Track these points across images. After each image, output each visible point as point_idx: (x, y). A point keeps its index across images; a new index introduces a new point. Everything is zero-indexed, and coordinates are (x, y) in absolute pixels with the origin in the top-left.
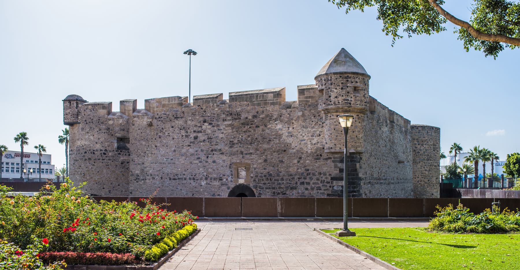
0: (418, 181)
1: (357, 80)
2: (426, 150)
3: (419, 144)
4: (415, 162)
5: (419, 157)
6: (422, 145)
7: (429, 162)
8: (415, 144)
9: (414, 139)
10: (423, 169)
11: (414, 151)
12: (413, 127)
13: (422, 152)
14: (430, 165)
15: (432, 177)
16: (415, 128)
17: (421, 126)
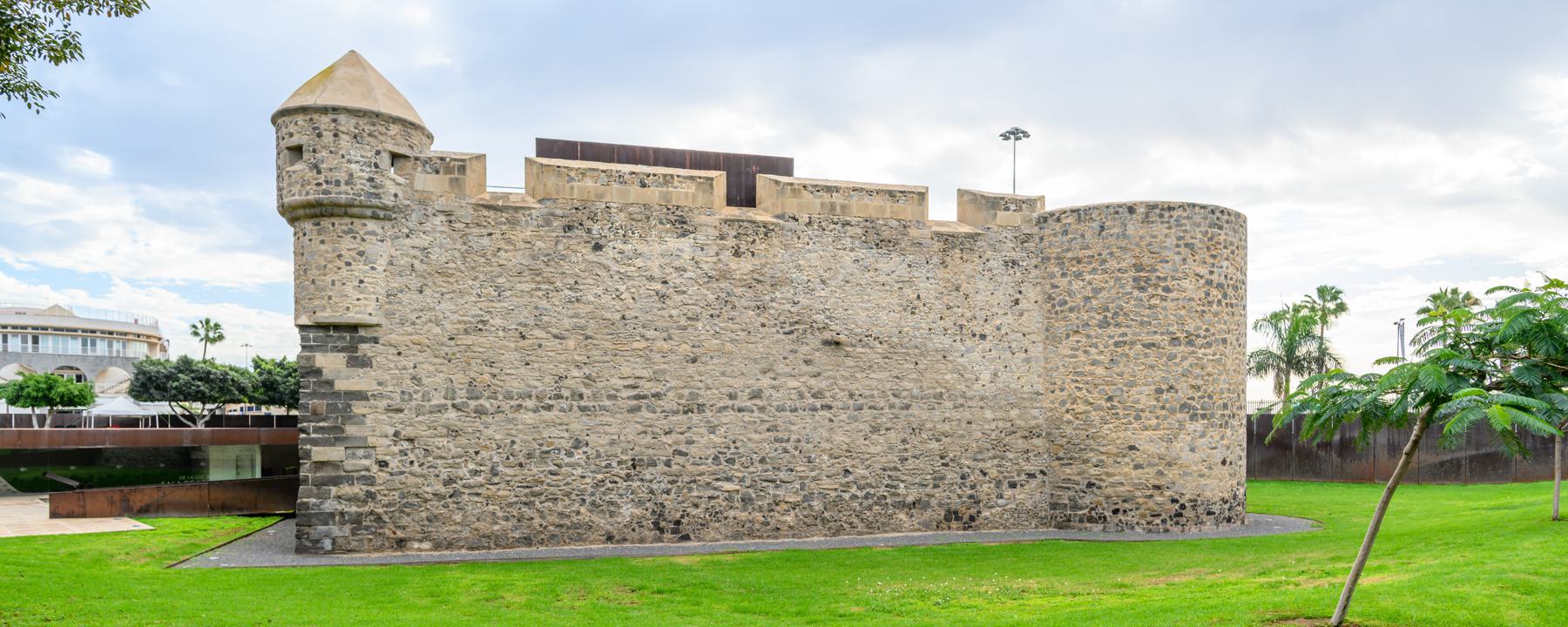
0: (1063, 403)
1: (292, 128)
2: (1097, 291)
3: (1064, 275)
4: (1051, 338)
5: (1064, 319)
6: (1078, 275)
7: (1111, 330)
8: (1052, 276)
9: (1048, 259)
10: (1083, 358)
11: (1050, 298)
12: (1043, 220)
13: (1079, 300)
14: (1116, 344)
15: (1131, 385)
16: (1050, 221)
17: (1073, 211)
